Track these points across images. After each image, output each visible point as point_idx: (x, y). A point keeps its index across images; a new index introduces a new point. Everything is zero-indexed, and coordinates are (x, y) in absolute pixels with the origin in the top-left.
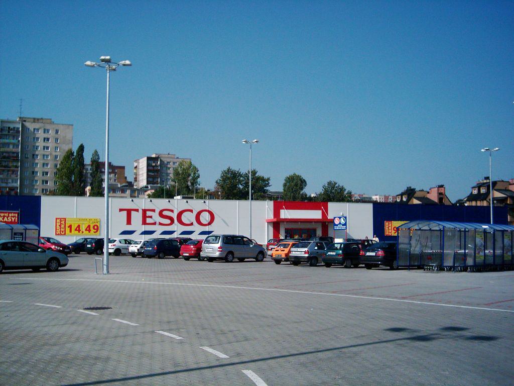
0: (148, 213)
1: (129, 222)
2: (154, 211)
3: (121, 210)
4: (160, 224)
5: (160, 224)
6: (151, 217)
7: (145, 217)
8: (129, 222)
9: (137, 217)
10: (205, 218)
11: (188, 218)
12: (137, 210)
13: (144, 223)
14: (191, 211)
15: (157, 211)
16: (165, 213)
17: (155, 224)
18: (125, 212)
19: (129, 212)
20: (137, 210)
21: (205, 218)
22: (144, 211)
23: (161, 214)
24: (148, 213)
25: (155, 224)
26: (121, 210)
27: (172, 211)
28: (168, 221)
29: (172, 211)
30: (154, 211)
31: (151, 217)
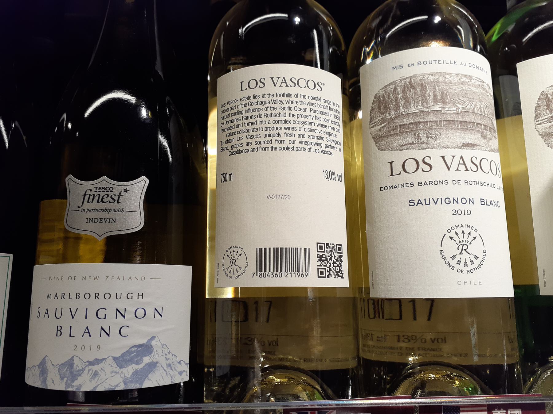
1: (96, 189)
3: (95, 187)
4: (102, 190)
5: (102, 190)
7: (99, 189)
8: (96, 189)
9: (98, 189)
11: (108, 189)
12: (98, 187)
13: (99, 190)
14: (108, 187)
17: (101, 190)
19: (96, 188)
20: (98, 187)
21: (111, 189)
22: (99, 187)
23: (102, 188)
25: (101, 190)
26: (95, 187)
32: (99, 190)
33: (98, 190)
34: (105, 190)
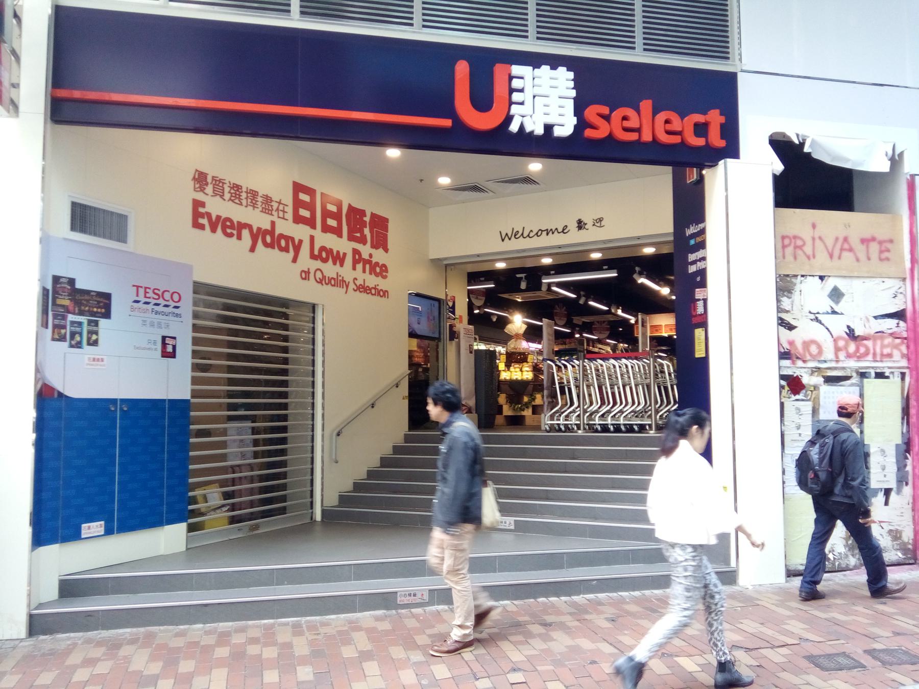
0: (148, 290)
1: (137, 295)
2: (149, 288)
3: (134, 286)
6: (148, 293)
7: (146, 292)
8: (137, 295)
10: (176, 297)
12: (141, 287)
13: (145, 297)
15: (152, 289)
16: (156, 291)
17: (149, 298)
18: (135, 288)
19: (138, 287)
20: (141, 287)
21: (176, 297)
22: (146, 288)
24: (148, 290)
25: (149, 298)
26: (134, 286)
27: (159, 290)
28: (156, 297)
29: (159, 290)
30: (149, 288)
31: (148, 293)
32: (145, 297)
33: (141, 298)
34: (161, 301)
